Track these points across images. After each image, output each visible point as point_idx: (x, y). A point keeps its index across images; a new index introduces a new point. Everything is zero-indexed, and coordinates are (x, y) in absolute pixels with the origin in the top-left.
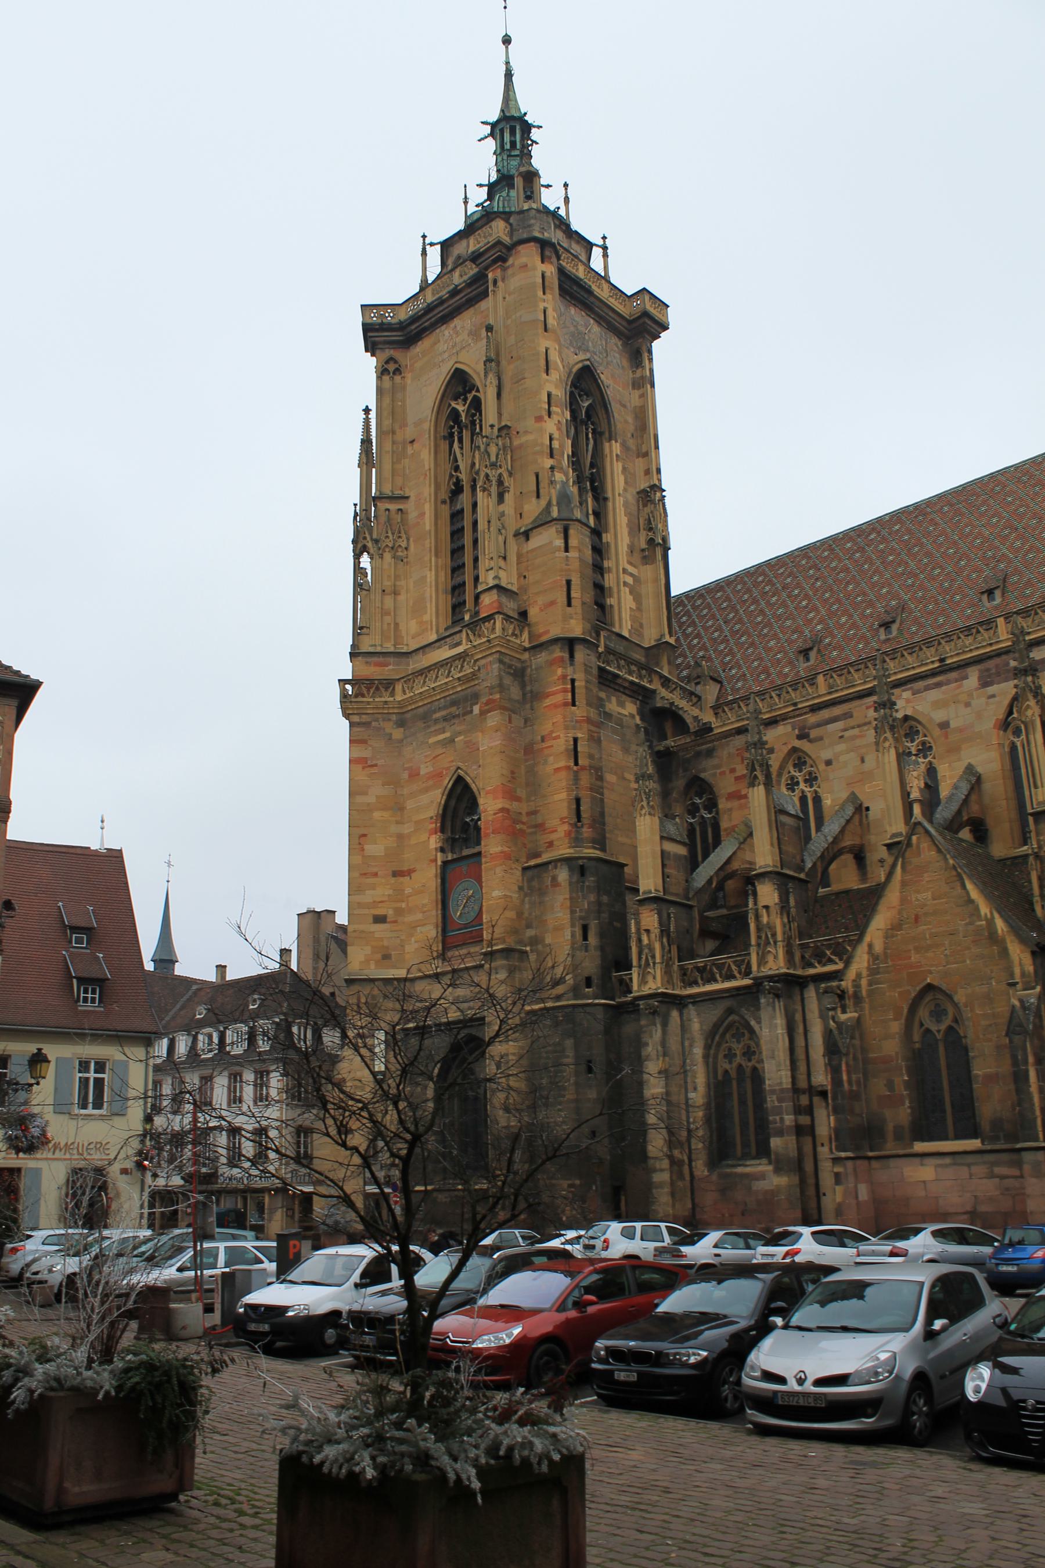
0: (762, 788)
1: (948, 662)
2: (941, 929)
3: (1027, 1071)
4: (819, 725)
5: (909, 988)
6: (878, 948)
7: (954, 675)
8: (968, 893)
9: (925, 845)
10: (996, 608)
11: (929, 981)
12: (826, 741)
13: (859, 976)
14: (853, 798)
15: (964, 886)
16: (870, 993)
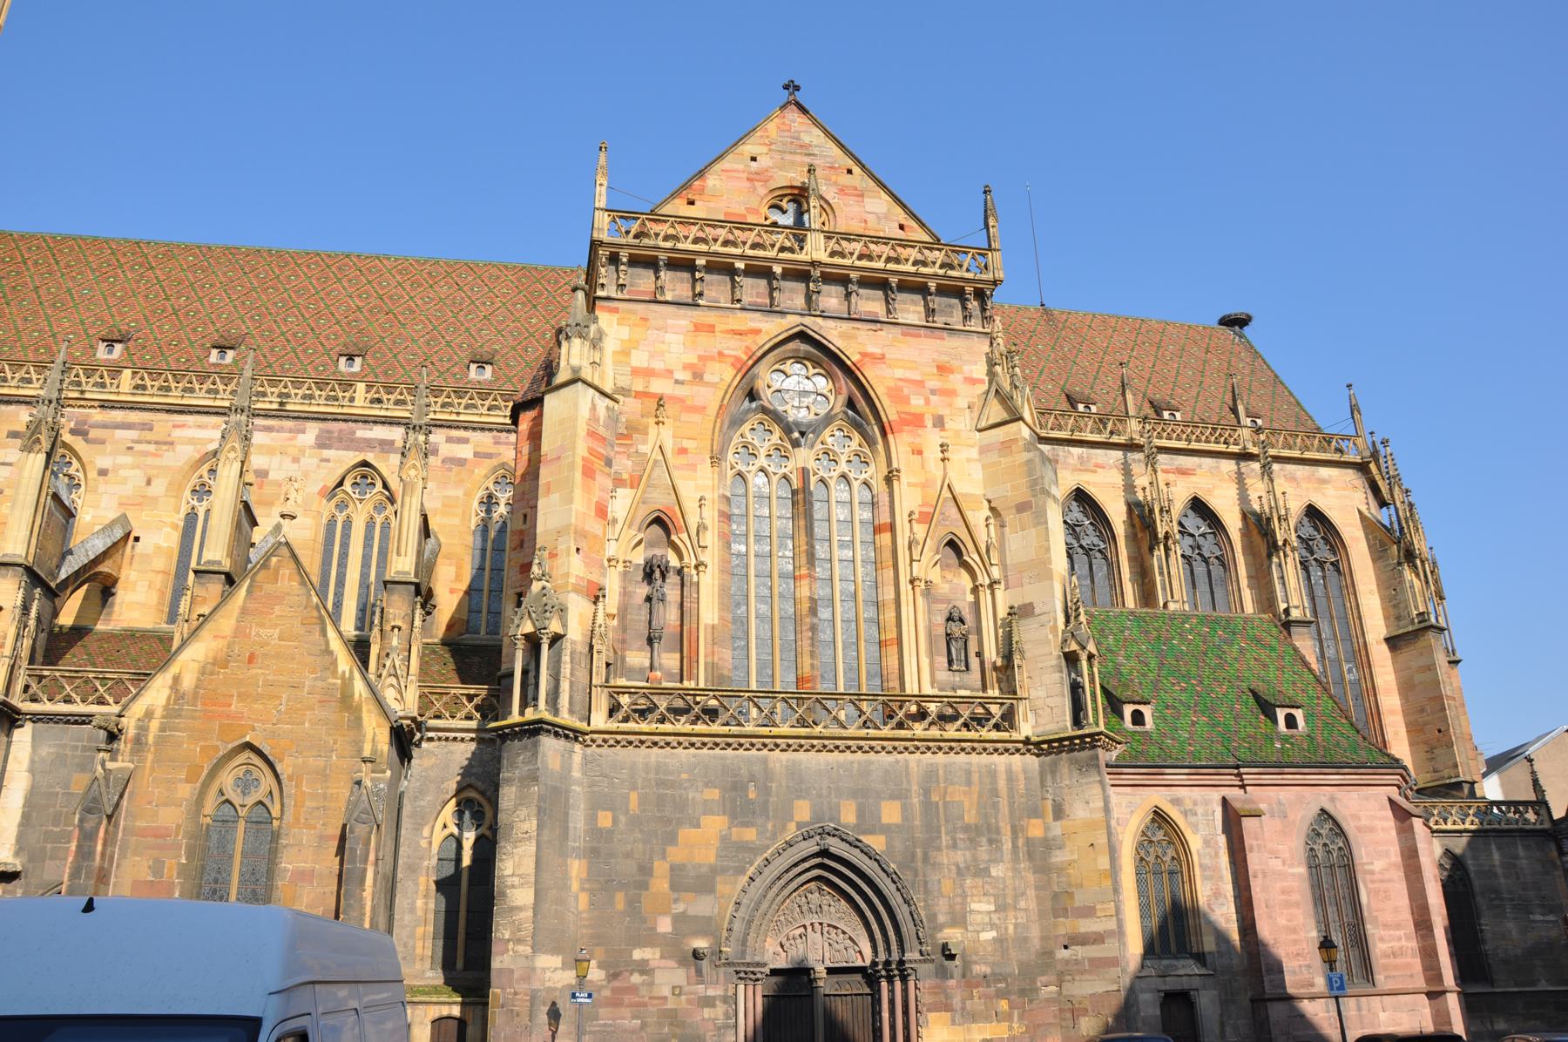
0: (42, 457)
1: (288, 407)
2: (282, 678)
3: (365, 870)
4: (105, 426)
5: (219, 743)
6: (188, 683)
7: (289, 424)
8: (327, 643)
9: (287, 572)
10: (353, 374)
11: (247, 739)
12: (109, 447)
13: (149, 714)
14: (123, 519)
15: (324, 633)
16: (161, 741)
